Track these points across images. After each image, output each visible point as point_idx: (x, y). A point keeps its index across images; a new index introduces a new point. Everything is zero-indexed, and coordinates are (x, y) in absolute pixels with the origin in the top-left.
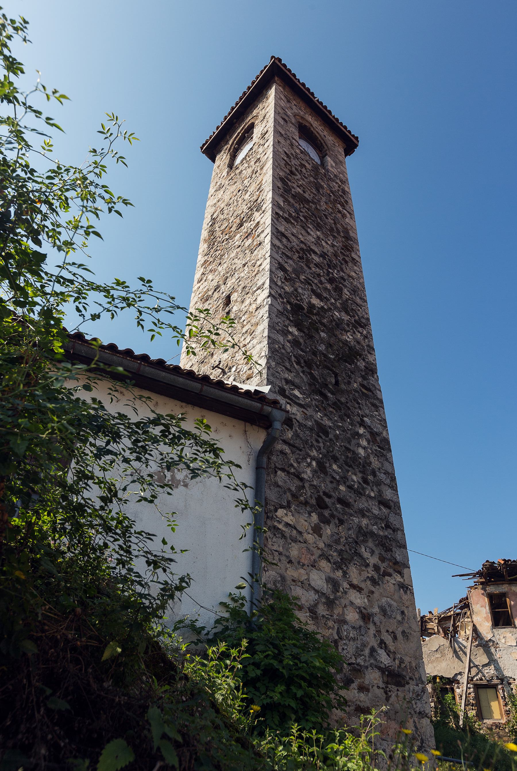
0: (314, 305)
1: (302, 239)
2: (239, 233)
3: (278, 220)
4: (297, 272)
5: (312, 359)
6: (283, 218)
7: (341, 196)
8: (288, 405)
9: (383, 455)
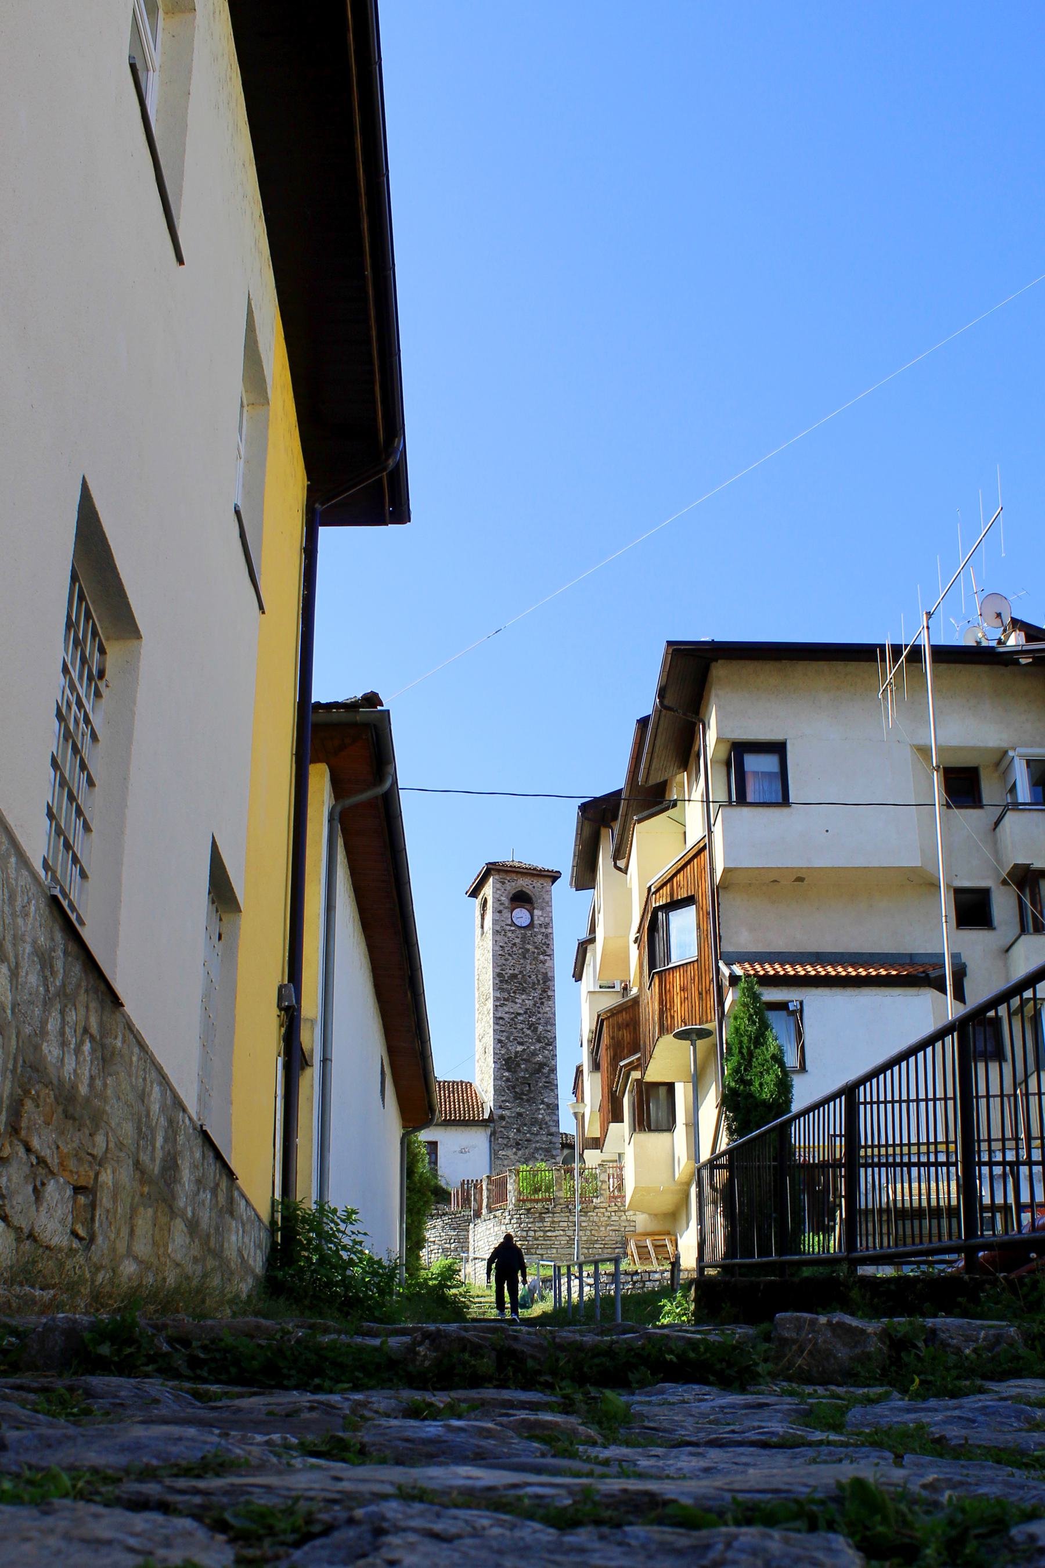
4: (508, 1038)
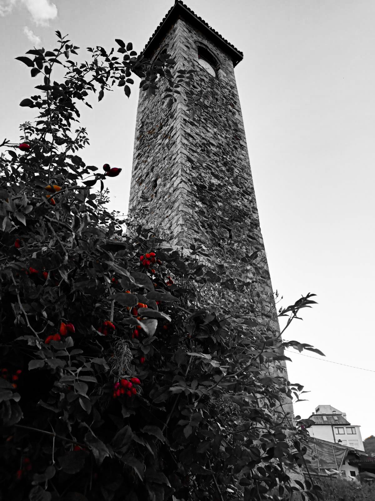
0: (213, 184)
1: (204, 136)
2: (160, 134)
3: (185, 125)
5: (213, 223)
6: (189, 122)
7: (231, 98)
8: (197, 256)
9: (264, 282)
